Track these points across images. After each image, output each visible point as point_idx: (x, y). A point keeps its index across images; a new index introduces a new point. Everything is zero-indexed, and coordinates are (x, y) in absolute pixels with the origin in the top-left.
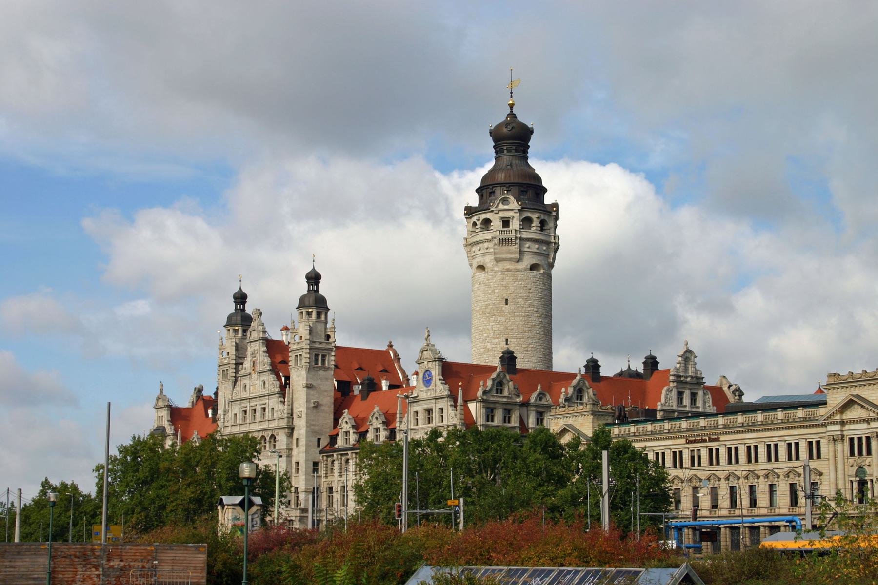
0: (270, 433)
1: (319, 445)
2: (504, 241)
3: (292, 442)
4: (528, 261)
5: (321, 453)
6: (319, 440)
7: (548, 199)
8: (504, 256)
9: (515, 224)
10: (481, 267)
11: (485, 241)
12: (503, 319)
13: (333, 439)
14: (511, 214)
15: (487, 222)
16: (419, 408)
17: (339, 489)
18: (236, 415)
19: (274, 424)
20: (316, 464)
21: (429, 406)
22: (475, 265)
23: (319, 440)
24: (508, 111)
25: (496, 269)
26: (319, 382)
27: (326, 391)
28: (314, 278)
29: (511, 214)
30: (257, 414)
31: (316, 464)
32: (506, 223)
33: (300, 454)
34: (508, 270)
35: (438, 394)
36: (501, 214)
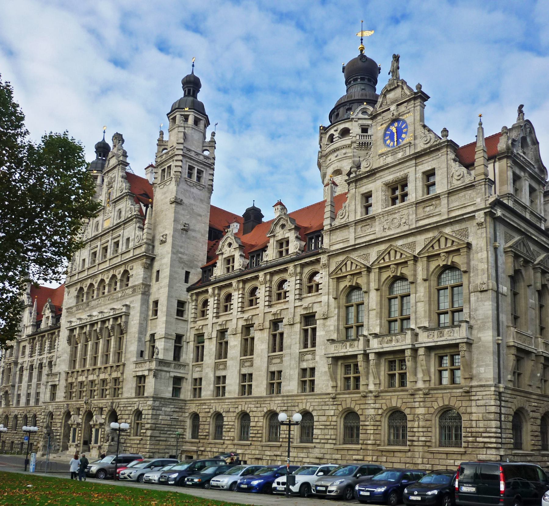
1: (186, 281)
3: (150, 277)
5: (189, 290)
6: (187, 273)
13: (208, 270)
15: (345, 132)
17: (214, 335)
18: (84, 260)
20: (181, 304)
22: (330, 171)
23: (187, 273)
26: (192, 201)
30: (109, 251)
31: (181, 304)
33: (160, 291)
36: (360, 122)
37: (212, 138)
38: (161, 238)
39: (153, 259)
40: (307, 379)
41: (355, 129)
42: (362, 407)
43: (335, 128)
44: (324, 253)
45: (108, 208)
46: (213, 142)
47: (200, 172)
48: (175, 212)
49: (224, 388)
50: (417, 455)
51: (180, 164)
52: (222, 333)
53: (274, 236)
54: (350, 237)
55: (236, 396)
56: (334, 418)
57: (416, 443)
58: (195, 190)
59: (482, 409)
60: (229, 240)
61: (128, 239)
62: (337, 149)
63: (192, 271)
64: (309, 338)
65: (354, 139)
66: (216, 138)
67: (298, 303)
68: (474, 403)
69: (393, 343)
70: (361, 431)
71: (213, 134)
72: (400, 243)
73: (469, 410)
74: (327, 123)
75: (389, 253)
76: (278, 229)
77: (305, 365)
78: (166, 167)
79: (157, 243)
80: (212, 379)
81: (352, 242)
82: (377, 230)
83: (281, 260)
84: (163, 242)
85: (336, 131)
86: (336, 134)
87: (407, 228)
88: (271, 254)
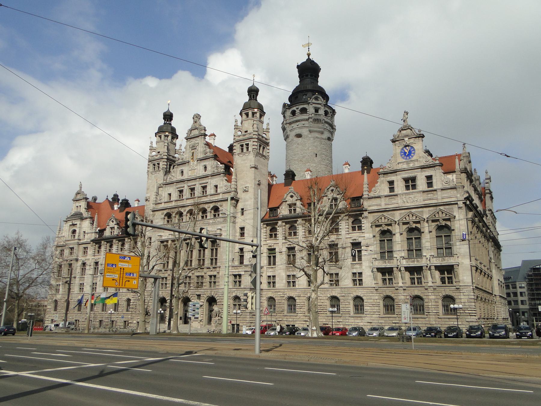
0: (212, 205)
2: (317, 121)
4: (326, 135)
8: (315, 129)
9: (321, 112)
10: (299, 136)
12: (314, 165)
14: (319, 106)
19: (220, 197)
24: (307, 58)
25: (310, 136)
27: (264, 175)
29: (319, 106)
32: (317, 110)
34: (317, 137)
35: (423, 163)
36: (314, 105)
38: (245, 189)
40: (357, 278)
41: (311, 109)
42: (396, 294)
43: (297, 107)
44: (366, 210)
45: (191, 163)
48: (255, 174)
50: (432, 319)
52: (291, 249)
53: (327, 196)
54: (383, 204)
55: (305, 287)
56: (378, 301)
57: (431, 314)
59: (467, 297)
62: (298, 121)
64: (357, 256)
65: (310, 116)
66: (270, 127)
67: (348, 236)
68: (462, 294)
69: (416, 263)
70: (396, 308)
73: (460, 297)
75: (409, 216)
77: (355, 271)
78: (244, 144)
80: (285, 277)
81: (383, 207)
84: (245, 191)
85: (297, 109)
86: (298, 111)
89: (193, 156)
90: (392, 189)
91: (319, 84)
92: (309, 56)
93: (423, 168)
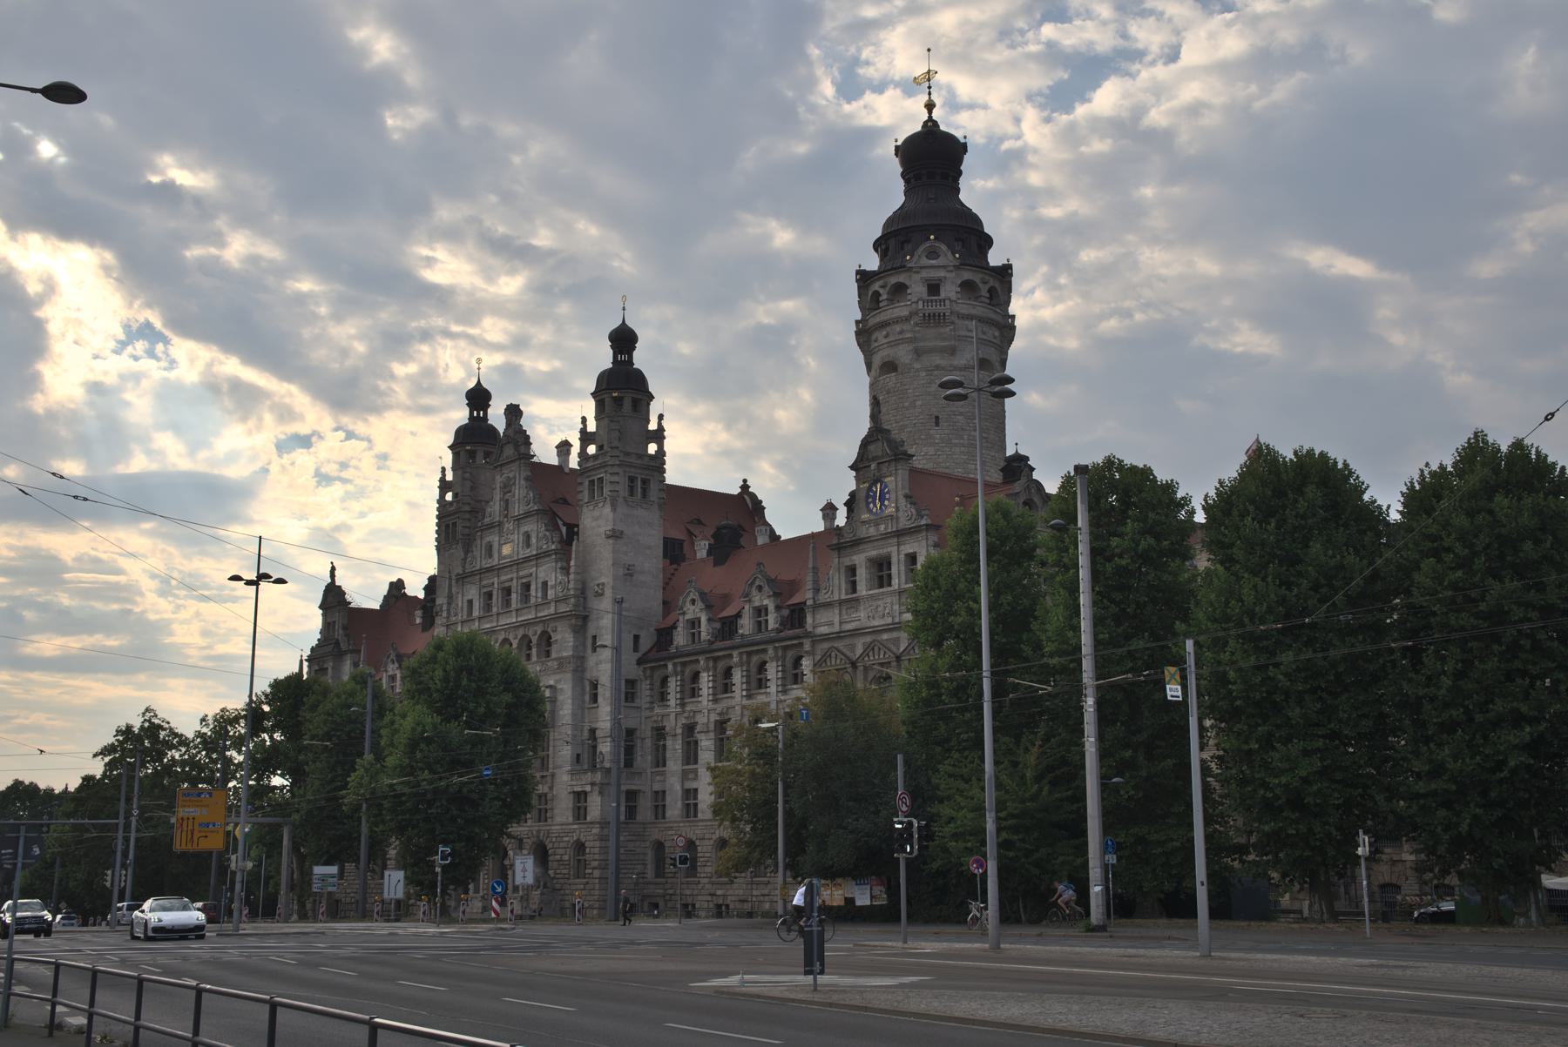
1: (636, 649)
2: (933, 319)
5: (639, 662)
6: (636, 638)
7: (995, 258)
9: (949, 290)
11: (898, 320)
12: (931, 450)
14: (942, 273)
15: (900, 289)
16: (860, 559)
18: (470, 602)
21: (883, 551)
23: (636, 638)
25: (917, 366)
28: (623, 340)
29: (942, 273)
32: (933, 288)
33: (602, 667)
36: (924, 274)
37: (660, 424)
39: (585, 618)
46: (661, 429)
47: (644, 482)
48: (614, 551)
49: (696, 805)
51: (616, 478)
52: (690, 729)
58: (640, 512)
60: (692, 596)
61: (545, 584)
63: (643, 634)
66: (664, 423)
71: (661, 417)
72: (885, 636)
74: (873, 263)
76: (754, 591)
79: (590, 595)
81: (836, 629)
82: (861, 617)
83: (759, 637)
87: (889, 620)
88: (746, 625)
89: (507, 508)
90: (853, 587)
91: (964, 197)
92: (930, 112)
93: (900, 534)
